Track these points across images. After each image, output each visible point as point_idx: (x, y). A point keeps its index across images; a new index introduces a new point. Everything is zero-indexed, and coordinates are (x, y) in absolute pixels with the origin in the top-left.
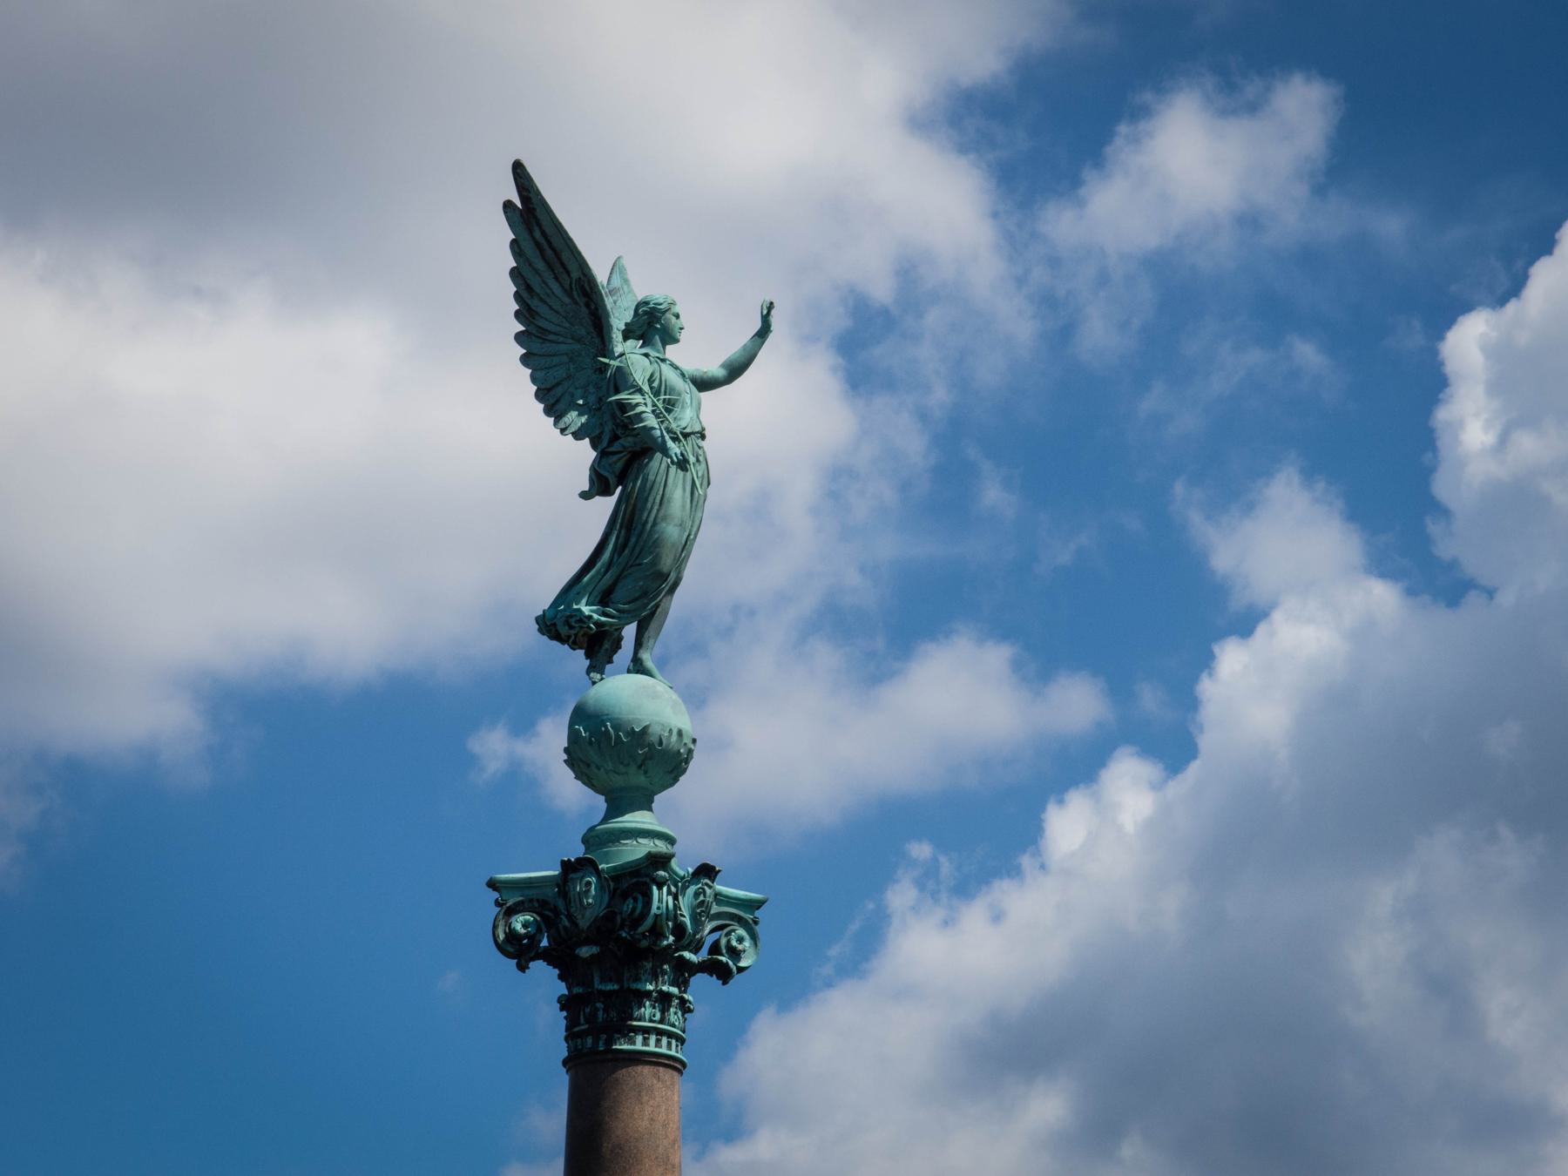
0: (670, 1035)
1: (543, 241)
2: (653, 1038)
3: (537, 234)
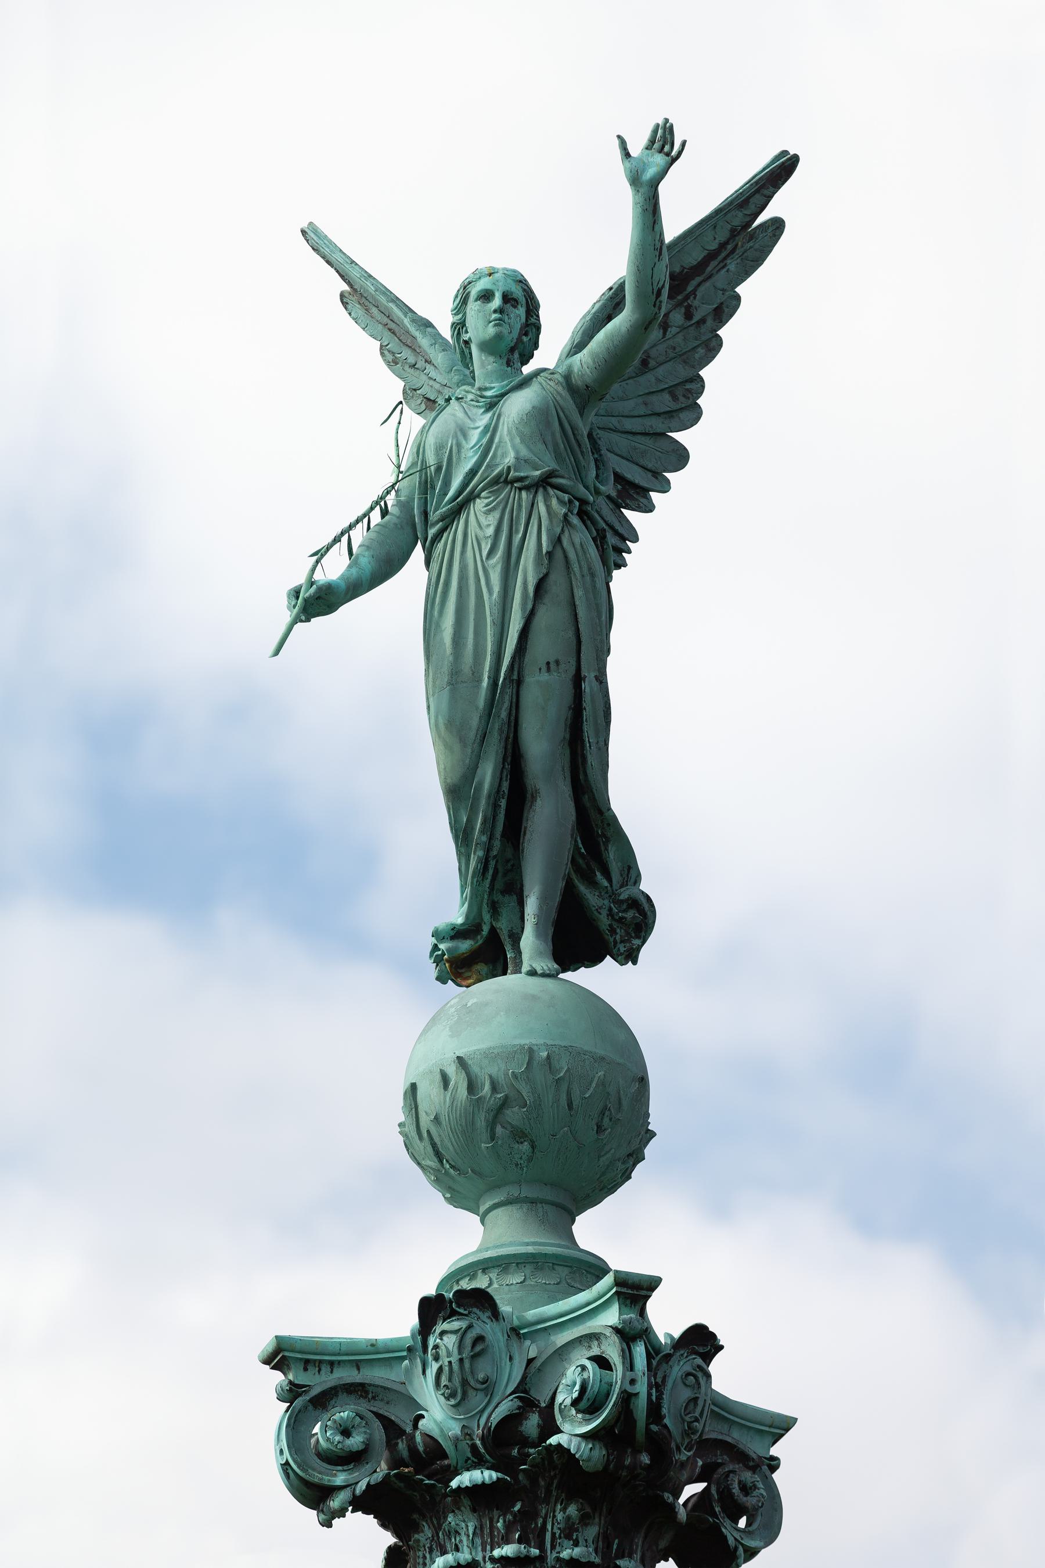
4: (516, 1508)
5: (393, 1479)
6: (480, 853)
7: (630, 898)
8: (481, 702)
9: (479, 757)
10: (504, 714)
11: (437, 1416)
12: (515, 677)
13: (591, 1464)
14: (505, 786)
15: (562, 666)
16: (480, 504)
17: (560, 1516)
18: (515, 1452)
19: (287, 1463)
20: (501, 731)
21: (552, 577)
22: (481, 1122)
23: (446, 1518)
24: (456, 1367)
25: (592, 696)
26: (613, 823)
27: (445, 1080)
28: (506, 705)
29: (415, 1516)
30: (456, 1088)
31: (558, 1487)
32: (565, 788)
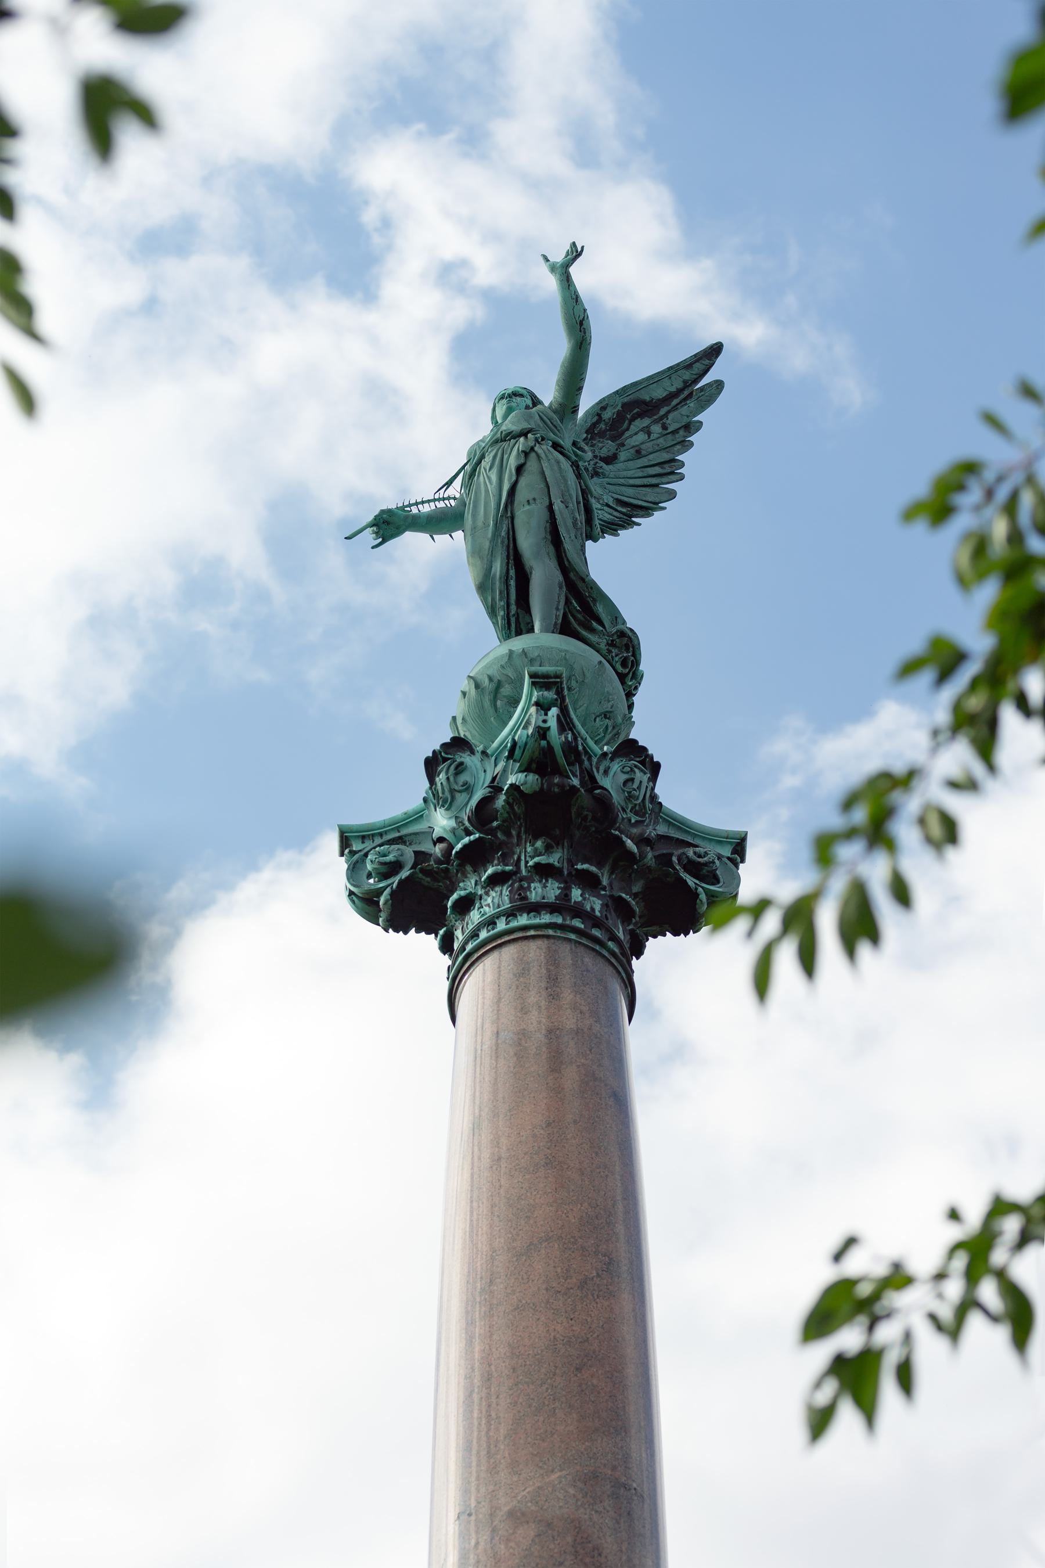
5: (420, 875)
6: (502, 613)
7: (618, 631)
8: (490, 535)
9: (491, 562)
10: (503, 534)
12: (509, 514)
13: (528, 785)
14: (512, 573)
15: (538, 501)
17: (529, 849)
20: (502, 542)
21: (528, 464)
22: (487, 703)
24: (445, 783)
25: (561, 512)
26: (593, 586)
28: (505, 528)
31: (526, 832)
32: (552, 565)
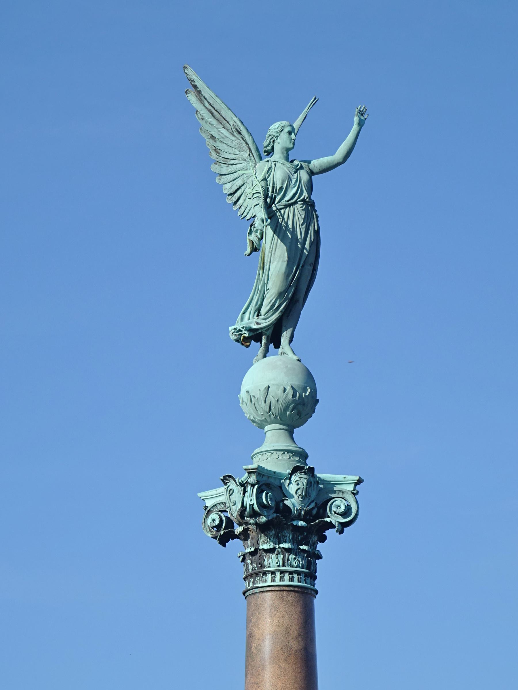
0: (291, 573)
1: (211, 108)
2: (278, 574)
3: (207, 104)
4: (305, 534)
11: (294, 502)
16: (299, 206)
18: (308, 517)
19: (253, 505)
23: (284, 530)
27: (285, 390)
29: (271, 527)
30: (287, 394)
